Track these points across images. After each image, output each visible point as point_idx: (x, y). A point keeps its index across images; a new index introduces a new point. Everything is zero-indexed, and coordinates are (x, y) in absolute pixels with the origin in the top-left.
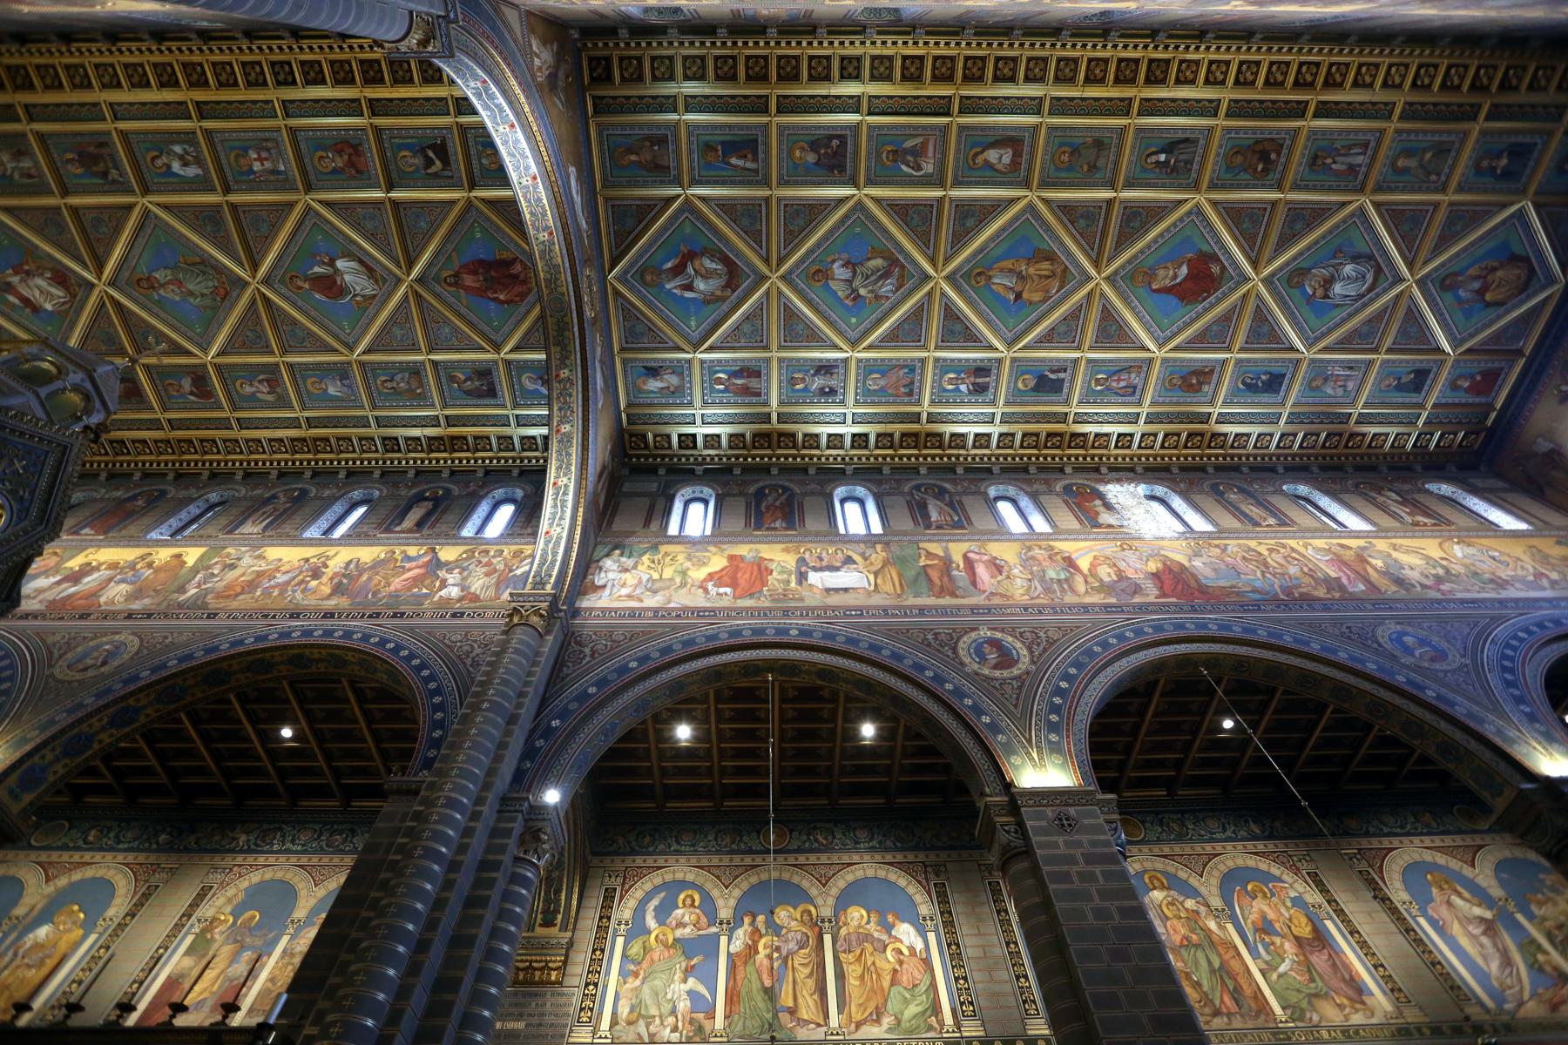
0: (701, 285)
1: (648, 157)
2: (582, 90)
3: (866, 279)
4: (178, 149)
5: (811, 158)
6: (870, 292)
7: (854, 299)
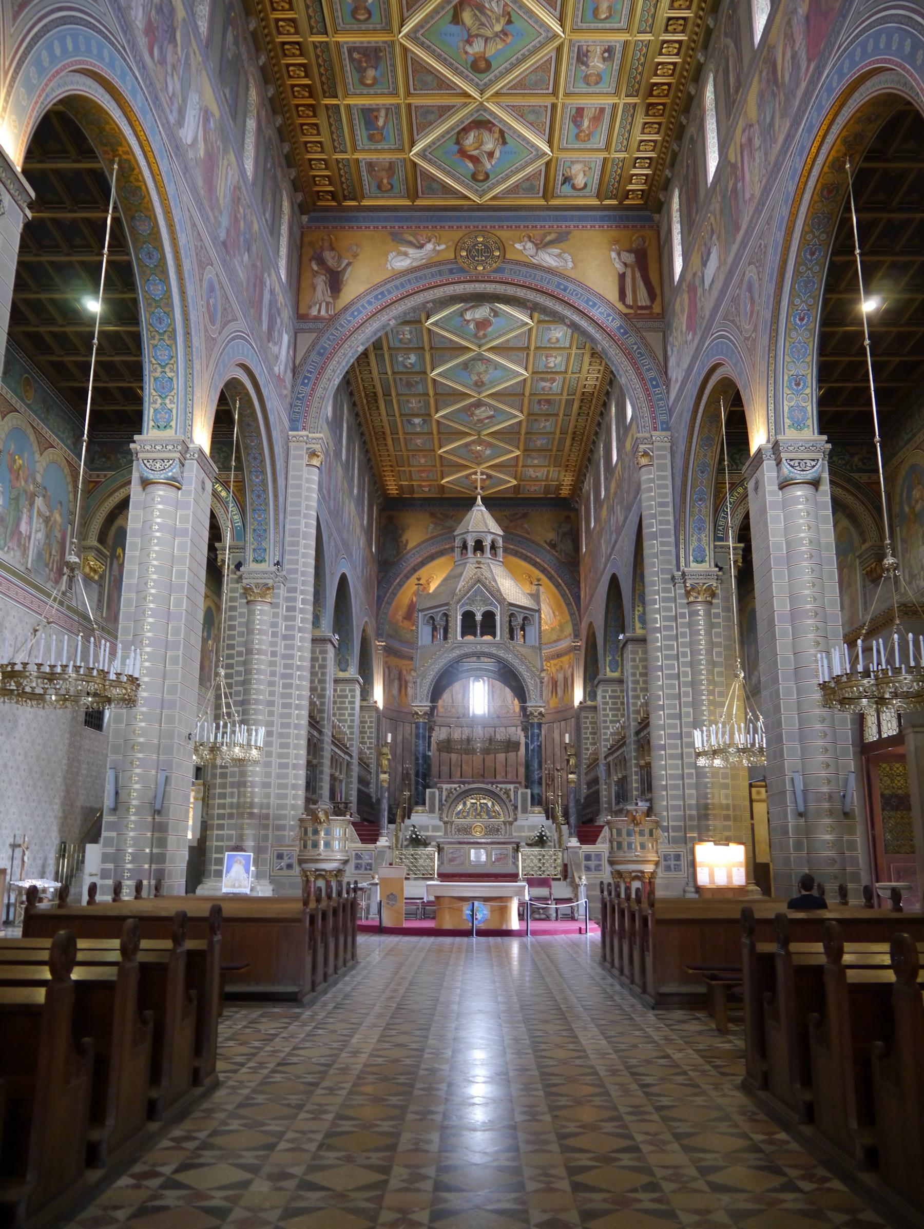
0: (489, 147)
1: (384, 173)
2: (341, 208)
3: (483, 24)
4: (401, 359)
5: (371, 73)
6: (498, 20)
7: (506, 34)
